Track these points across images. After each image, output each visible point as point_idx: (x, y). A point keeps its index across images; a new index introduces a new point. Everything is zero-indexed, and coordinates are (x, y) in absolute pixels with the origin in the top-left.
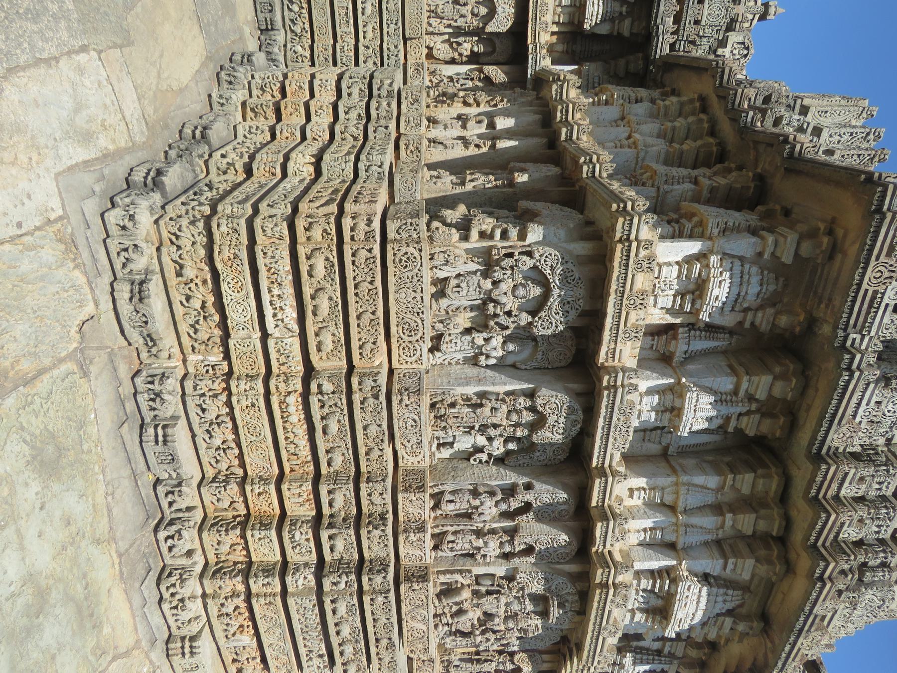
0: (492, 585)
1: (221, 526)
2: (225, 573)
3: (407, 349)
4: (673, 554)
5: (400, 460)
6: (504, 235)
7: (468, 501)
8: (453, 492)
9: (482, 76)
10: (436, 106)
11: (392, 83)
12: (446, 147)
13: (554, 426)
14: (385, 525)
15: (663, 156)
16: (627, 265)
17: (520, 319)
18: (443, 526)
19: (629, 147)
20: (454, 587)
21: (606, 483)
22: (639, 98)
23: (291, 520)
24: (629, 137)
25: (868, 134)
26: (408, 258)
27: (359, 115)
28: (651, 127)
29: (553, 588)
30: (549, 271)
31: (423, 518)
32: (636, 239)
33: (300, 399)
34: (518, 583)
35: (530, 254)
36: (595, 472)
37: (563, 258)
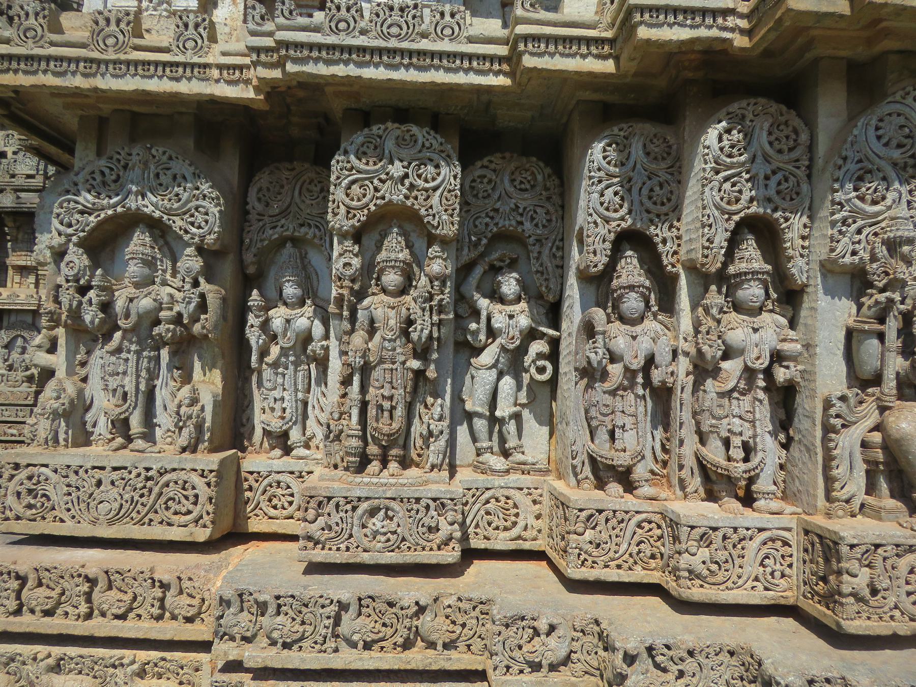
0: (881, 336)
3: (275, 501)
5: (527, 546)
7: (613, 393)
13: (412, 187)
16: (29, 58)
17: (189, 271)
18: (681, 467)
20: (880, 455)
21: (536, 38)
26: (30, 491)
29: (896, 154)
30: (92, 218)
31: (657, 518)
34: (874, 258)
35: (59, 254)
37: (68, 192)
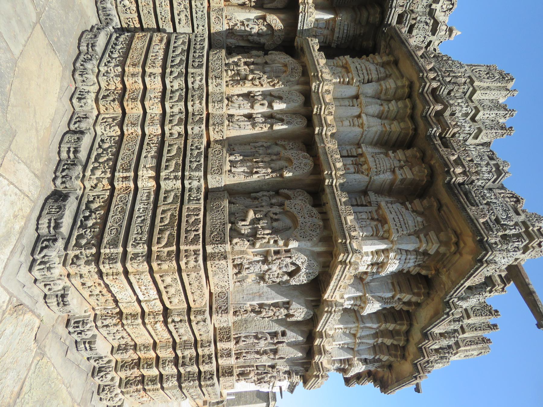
1: (126, 367)
2: (131, 384)
4: (351, 352)
6: (276, 242)
8: (246, 337)
9: (265, 23)
10: (233, 86)
11: (202, 79)
12: (240, 127)
14: (211, 363)
15: (378, 133)
19: (358, 126)
22: (370, 79)
23: (163, 361)
24: (359, 116)
25: (506, 114)
27: (180, 109)
28: (374, 109)
32: (350, 262)
33: (162, 324)
36: (317, 334)
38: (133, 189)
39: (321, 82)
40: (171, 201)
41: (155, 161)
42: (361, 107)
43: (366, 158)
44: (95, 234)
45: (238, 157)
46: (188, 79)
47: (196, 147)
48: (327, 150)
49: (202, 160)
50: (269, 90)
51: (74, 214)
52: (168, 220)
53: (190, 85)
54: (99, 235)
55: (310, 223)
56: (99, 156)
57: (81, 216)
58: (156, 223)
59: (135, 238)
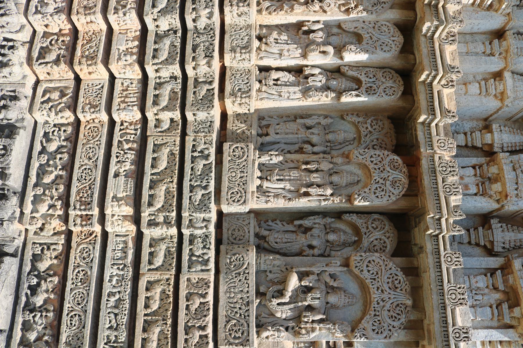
12: (281, 96)
24: (498, 75)
38: (99, 235)
39: (441, 23)
40: (160, 264)
41: (131, 183)
42: (505, 58)
43: (501, 169)
44: (49, 321)
45: (274, 158)
46: (186, 16)
47: (201, 152)
48: (437, 164)
49: (212, 183)
50: (339, 20)
51: (14, 283)
52: (158, 302)
53: (190, 24)
54: (55, 320)
55: (391, 302)
56: (42, 172)
57: (26, 286)
58: (138, 309)
59: (108, 337)
